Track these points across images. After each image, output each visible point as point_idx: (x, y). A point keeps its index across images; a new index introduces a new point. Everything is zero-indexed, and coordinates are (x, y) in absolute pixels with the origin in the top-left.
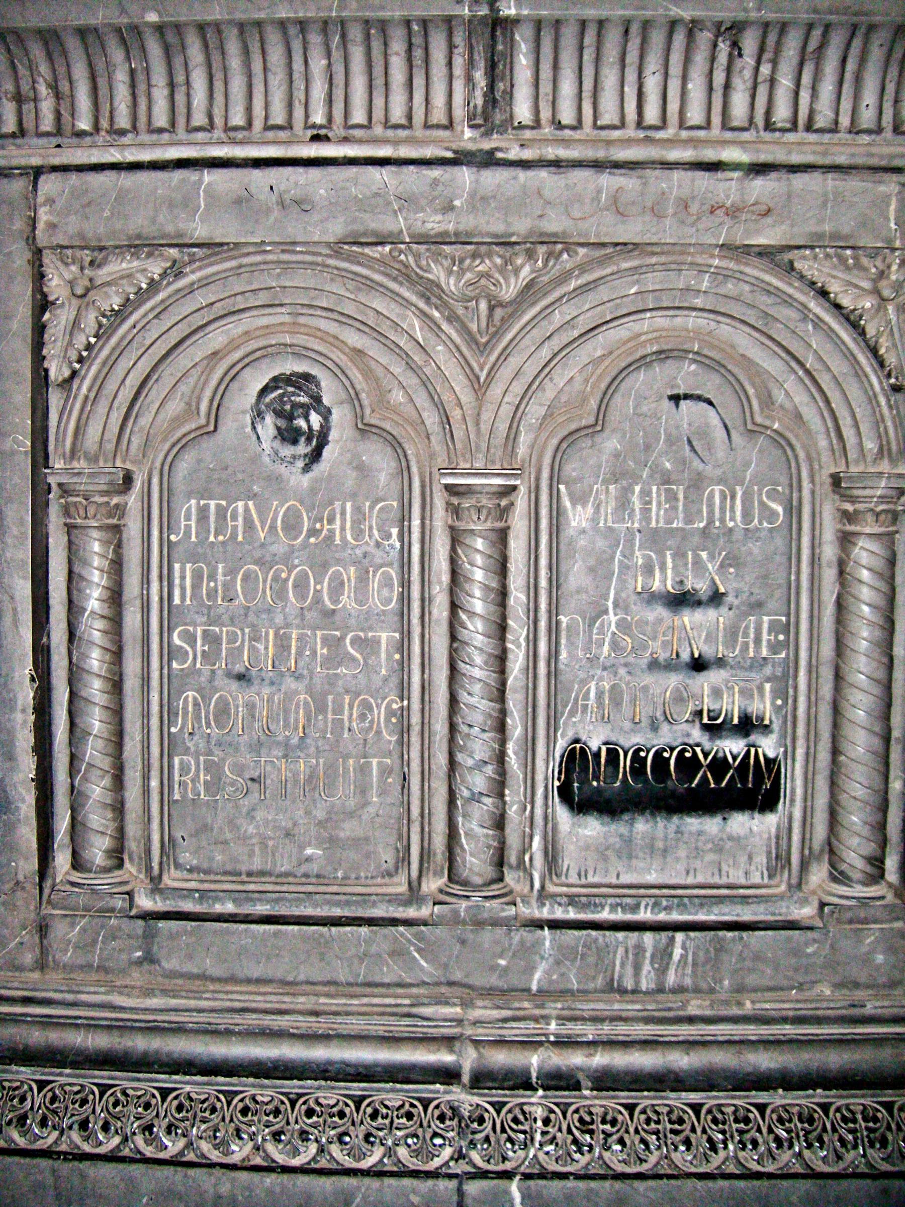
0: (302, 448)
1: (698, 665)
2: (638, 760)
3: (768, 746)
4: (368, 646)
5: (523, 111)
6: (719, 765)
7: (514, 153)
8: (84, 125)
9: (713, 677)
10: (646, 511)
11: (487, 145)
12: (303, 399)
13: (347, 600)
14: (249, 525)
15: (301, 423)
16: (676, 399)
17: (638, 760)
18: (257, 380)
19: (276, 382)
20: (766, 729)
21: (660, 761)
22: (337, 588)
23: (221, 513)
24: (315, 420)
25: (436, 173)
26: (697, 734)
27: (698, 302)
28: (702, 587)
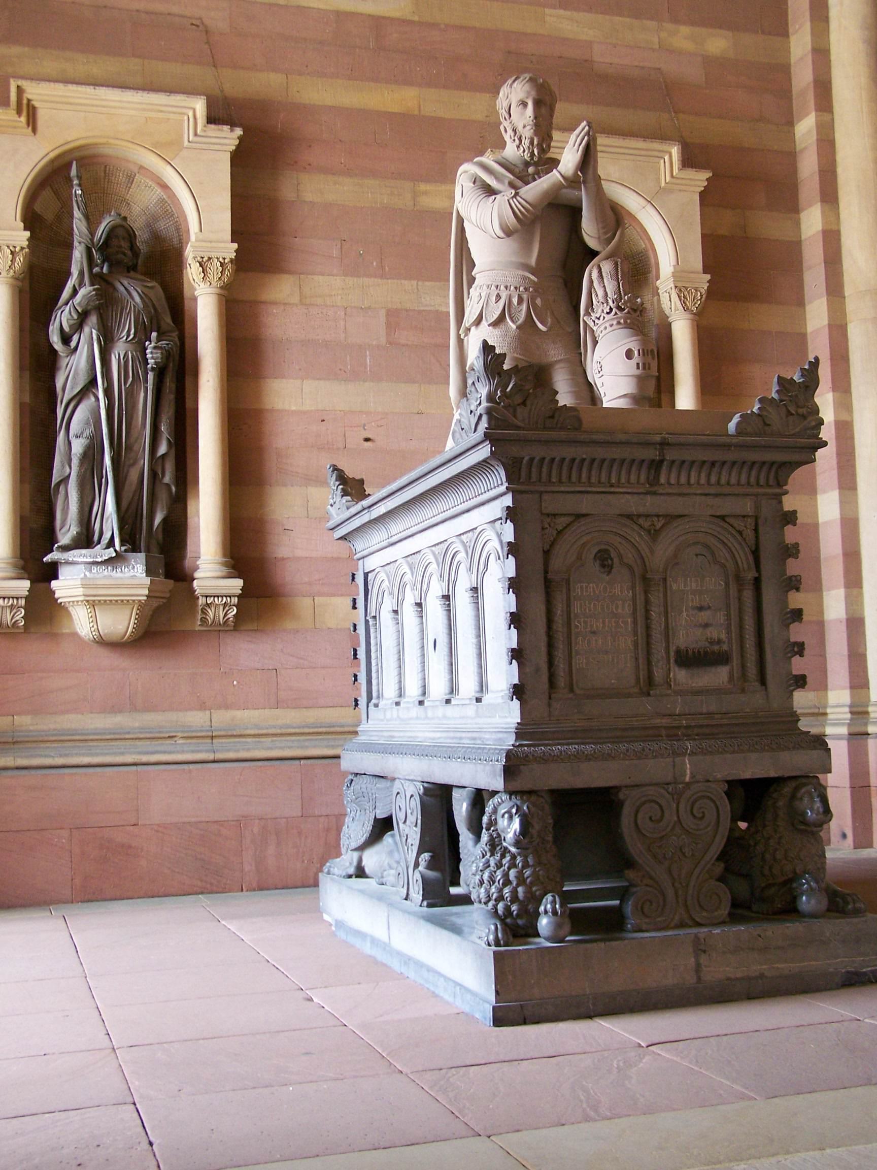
0: (606, 569)
1: (706, 626)
2: (694, 652)
3: (725, 647)
4: (626, 623)
5: (663, 480)
6: (713, 653)
7: (661, 491)
8: (554, 480)
9: (710, 629)
10: (691, 586)
11: (653, 489)
12: (606, 556)
13: (620, 611)
14: (594, 591)
15: (606, 563)
16: (697, 555)
17: (694, 652)
18: (595, 550)
19: (599, 551)
20: (724, 642)
21: (699, 652)
22: (617, 608)
23: (586, 587)
24: (610, 561)
25: (641, 496)
26: (707, 644)
27: (703, 530)
28: (705, 604)
